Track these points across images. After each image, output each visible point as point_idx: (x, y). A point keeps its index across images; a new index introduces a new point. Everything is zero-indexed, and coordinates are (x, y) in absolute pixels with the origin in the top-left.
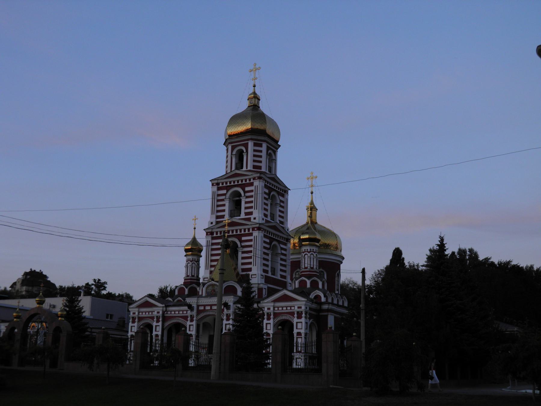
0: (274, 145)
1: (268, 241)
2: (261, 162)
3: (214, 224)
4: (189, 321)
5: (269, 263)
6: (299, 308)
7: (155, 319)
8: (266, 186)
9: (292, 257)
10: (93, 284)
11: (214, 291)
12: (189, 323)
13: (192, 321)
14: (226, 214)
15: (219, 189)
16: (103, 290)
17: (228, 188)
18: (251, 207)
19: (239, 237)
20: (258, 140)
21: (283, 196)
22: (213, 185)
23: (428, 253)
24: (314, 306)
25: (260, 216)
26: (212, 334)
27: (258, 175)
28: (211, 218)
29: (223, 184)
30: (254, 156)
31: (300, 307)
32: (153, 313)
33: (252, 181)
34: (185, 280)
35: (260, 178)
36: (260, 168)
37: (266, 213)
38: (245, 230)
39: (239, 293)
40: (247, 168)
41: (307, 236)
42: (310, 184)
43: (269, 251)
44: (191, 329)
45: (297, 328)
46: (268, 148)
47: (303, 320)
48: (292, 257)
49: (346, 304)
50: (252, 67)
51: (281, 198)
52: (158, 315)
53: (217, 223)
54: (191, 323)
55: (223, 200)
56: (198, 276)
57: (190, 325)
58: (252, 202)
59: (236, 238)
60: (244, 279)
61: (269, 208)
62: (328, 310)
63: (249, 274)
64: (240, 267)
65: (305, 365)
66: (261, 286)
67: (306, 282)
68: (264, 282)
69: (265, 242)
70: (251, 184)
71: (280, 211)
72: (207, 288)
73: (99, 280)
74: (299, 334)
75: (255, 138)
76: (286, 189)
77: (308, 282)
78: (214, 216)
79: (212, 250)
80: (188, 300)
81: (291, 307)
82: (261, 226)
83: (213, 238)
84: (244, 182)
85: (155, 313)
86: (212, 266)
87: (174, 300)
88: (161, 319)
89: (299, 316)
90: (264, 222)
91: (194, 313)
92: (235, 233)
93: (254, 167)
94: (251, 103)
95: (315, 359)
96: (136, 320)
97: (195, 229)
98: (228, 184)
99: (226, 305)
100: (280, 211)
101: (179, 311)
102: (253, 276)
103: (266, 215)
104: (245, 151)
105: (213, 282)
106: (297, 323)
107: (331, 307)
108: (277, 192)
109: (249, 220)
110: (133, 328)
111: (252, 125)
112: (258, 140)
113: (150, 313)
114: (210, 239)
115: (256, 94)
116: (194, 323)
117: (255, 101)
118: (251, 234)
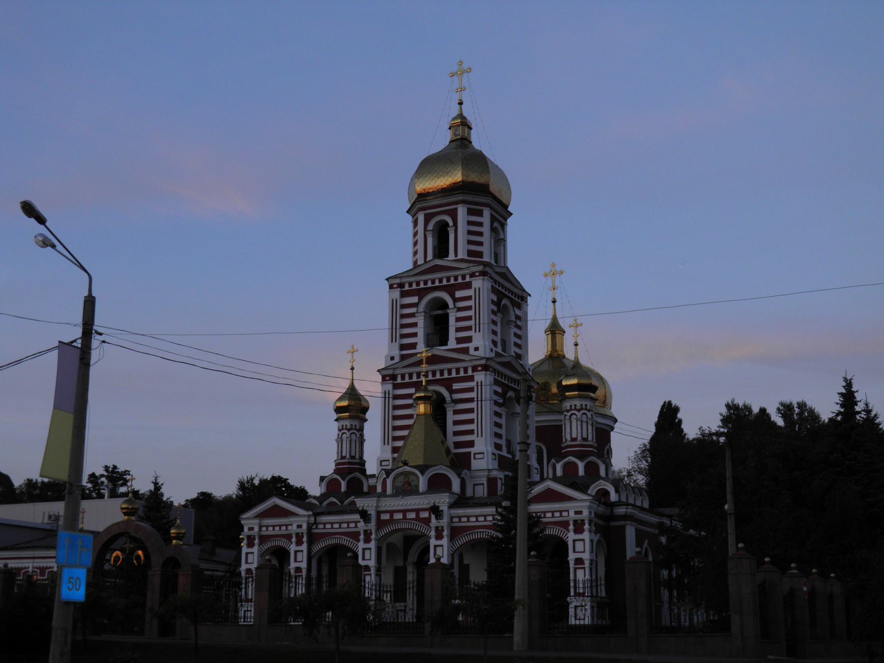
0: (501, 214)
1: (499, 390)
2: (480, 244)
3: (397, 359)
4: (362, 542)
5: (503, 432)
6: (576, 513)
7: (294, 540)
8: (494, 290)
9: (537, 419)
10: (102, 476)
11: (409, 484)
12: (361, 545)
13: (367, 540)
14: (420, 340)
15: (404, 294)
16: (122, 485)
17: (421, 293)
18: (469, 328)
19: (447, 383)
20: (476, 204)
21: (519, 306)
22: (391, 287)
23: (724, 411)
24: (601, 509)
25: (487, 343)
26: (400, 563)
27: (481, 268)
28: (390, 349)
29: (410, 285)
30: (470, 233)
31: (580, 513)
32: (290, 528)
33: (468, 279)
34: (336, 465)
35: (483, 274)
36: (480, 254)
37: (495, 338)
38: (458, 371)
39: (456, 486)
40: (456, 256)
41: (574, 381)
42: (550, 285)
43: (503, 408)
44: (367, 556)
45: (574, 551)
46: (493, 219)
47: (586, 535)
48: (537, 419)
49: (646, 505)
50: (455, 68)
51: (518, 312)
52: (299, 530)
53: (403, 357)
54: (367, 546)
55: (412, 315)
56: (361, 457)
57: (296, 552)
58: (469, 318)
59: (442, 385)
60: (461, 463)
61: (498, 329)
62: (626, 517)
63: (470, 453)
64: (451, 439)
65: (593, 619)
66: (495, 474)
67: (576, 466)
68: (497, 467)
69: (496, 393)
70: (468, 286)
71: (516, 335)
73: (115, 467)
74: (579, 561)
75: (463, 200)
76: (525, 295)
77: (581, 466)
78: (396, 345)
79: (396, 407)
80: (361, 503)
81: (561, 512)
82: (489, 363)
83: (396, 386)
84: (452, 281)
85: (293, 528)
86: (395, 439)
87: (342, 502)
88: (305, 539)
89: (579, 528)
90: (493, 355)
91: (372, 526)
92: (438, 376)
93: (470, 253)
94: (455, 135)
95: (611, 608)
96: (256, 541)
97: (352, 369)
98: (422, 286)
99: (435, 510)
100: (516, 335)
101: (340, 523)
102: (477, 456)
103: (494, 343)
104: (451, 223)
105: (407, 468)
106: (574, 541)
107: (630, 510)
108: (510, 298)
109: (466, 351)
110: (251, 559)
111: (463, 174)
112: (476, 204)
113: (284, 528)
115: (465, 118)
116: (372, 545)
117: (463, 131)
118: (471, 379)
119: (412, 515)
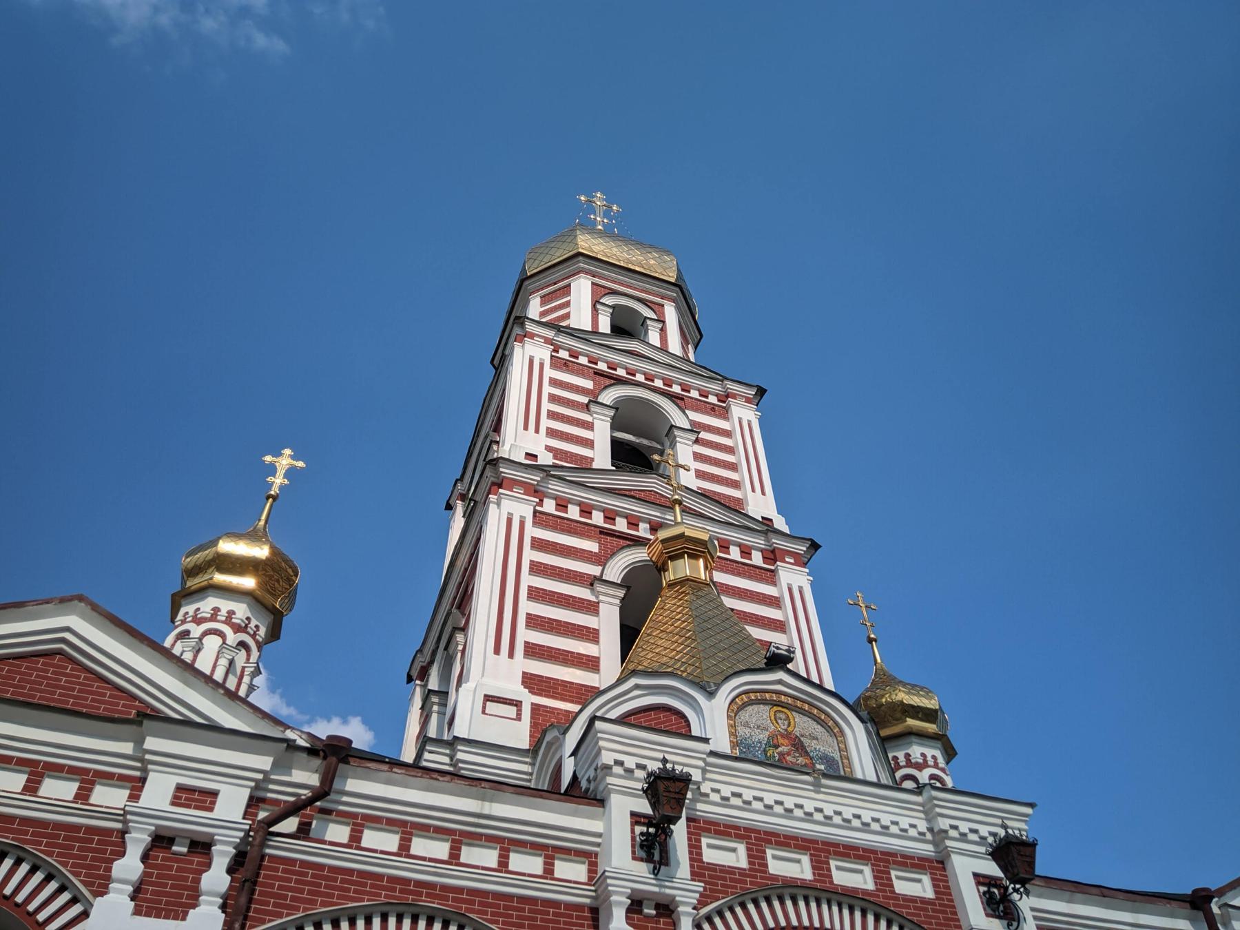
72: (736, 708)
83: (540, 519)
101: (459, 839)
114: (527, 511)
118: (769, 576)
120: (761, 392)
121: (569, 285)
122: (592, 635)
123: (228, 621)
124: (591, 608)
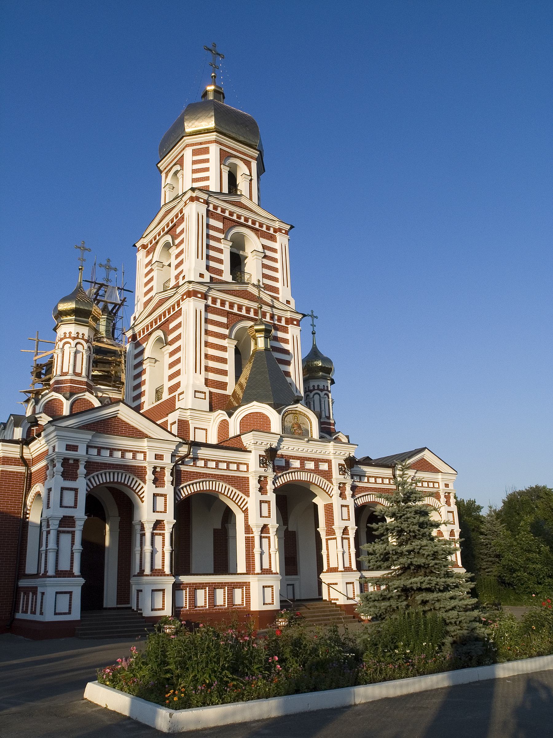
11: (299, 427)
33: (271, 231)
52: (159, 463)
72: (283, 415)
96: (82, 470)
119: (311, 465)
120: (292, 227)
121: (208, 148)
122: (224, 361)
123: (83, 339)
124: (224, 349)
